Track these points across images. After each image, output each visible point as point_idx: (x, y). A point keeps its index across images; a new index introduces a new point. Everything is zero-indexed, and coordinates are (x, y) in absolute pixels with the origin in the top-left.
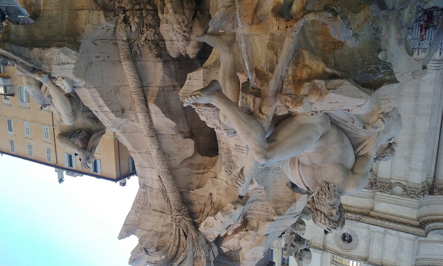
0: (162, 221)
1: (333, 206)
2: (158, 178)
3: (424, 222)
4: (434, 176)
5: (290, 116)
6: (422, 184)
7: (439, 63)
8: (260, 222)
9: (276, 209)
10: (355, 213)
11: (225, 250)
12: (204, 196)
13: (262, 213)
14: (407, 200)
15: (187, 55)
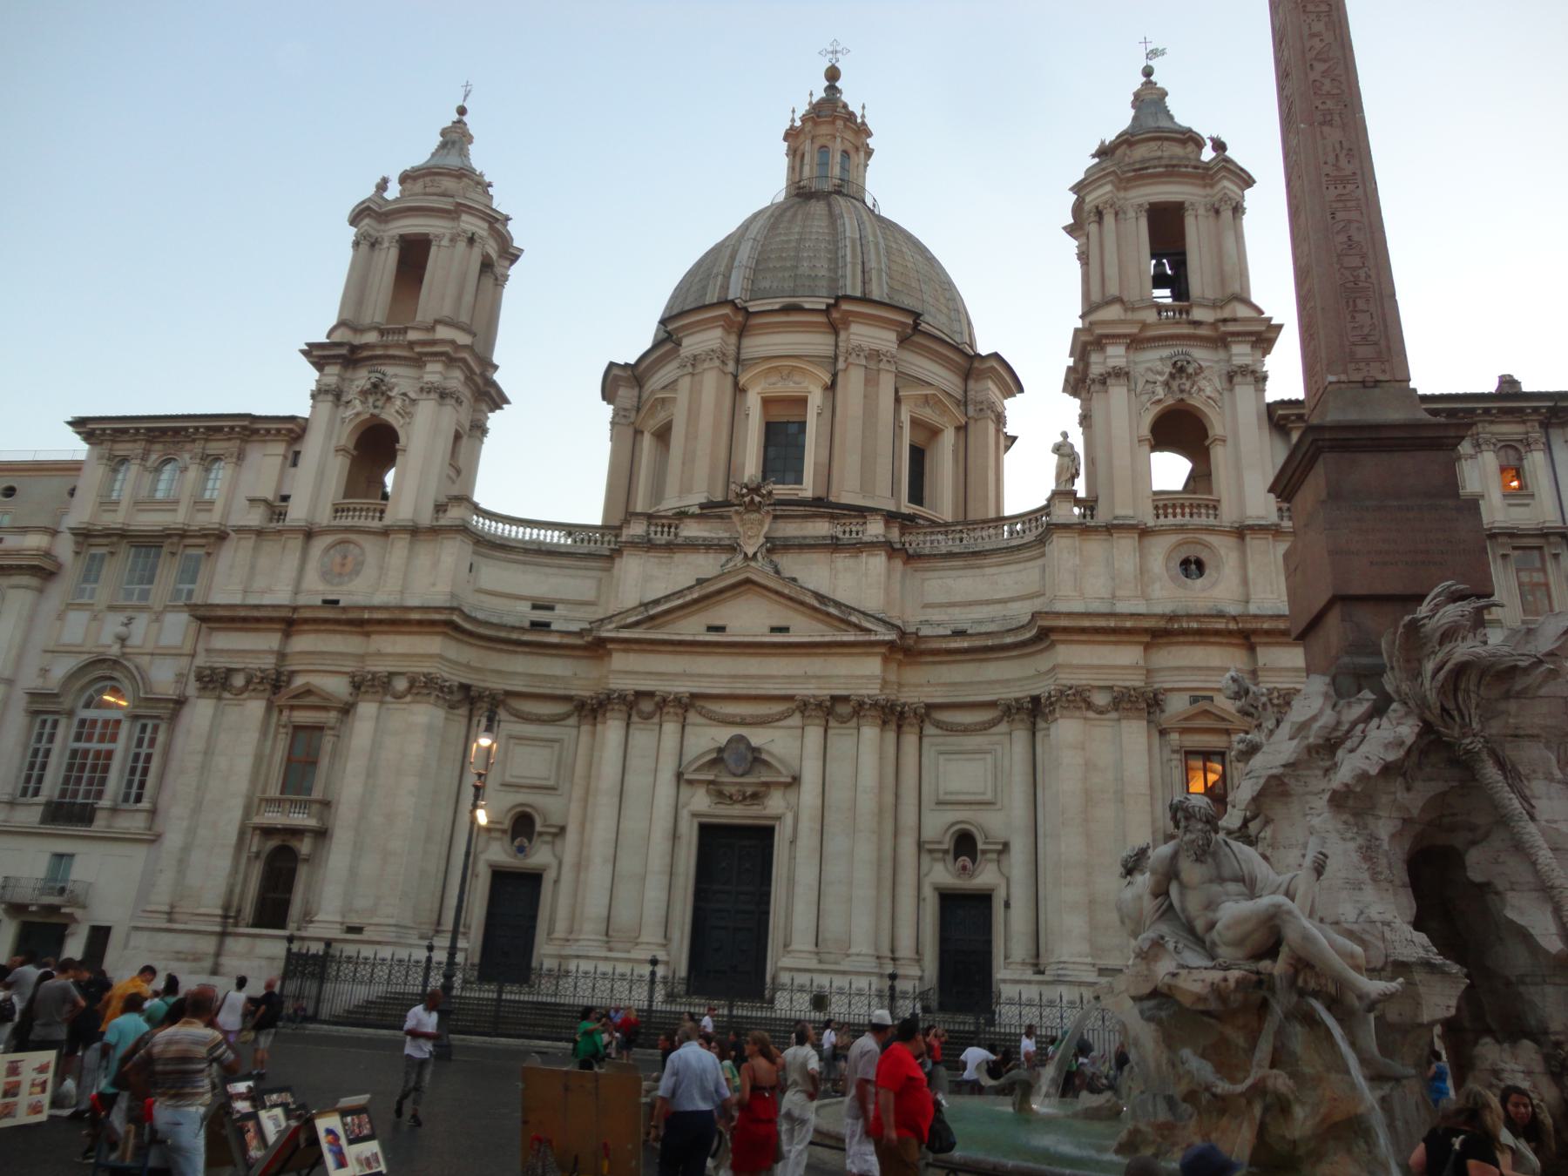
0: (1511, 721)
1: (1187, 829)
2: (1534, 802)
3: (1041, 640)
4: (1034, 734)
5: (1257, 956)
6: (1056, 719)
7: (1059, 975)
8: (1306, 757)
9: (1283, 784)
10: (1184, 632)
11: (1367, 694)
12: (1424, 781)
13: (1305, 773)
14: (1081, 679)
15: (1498, 1042)
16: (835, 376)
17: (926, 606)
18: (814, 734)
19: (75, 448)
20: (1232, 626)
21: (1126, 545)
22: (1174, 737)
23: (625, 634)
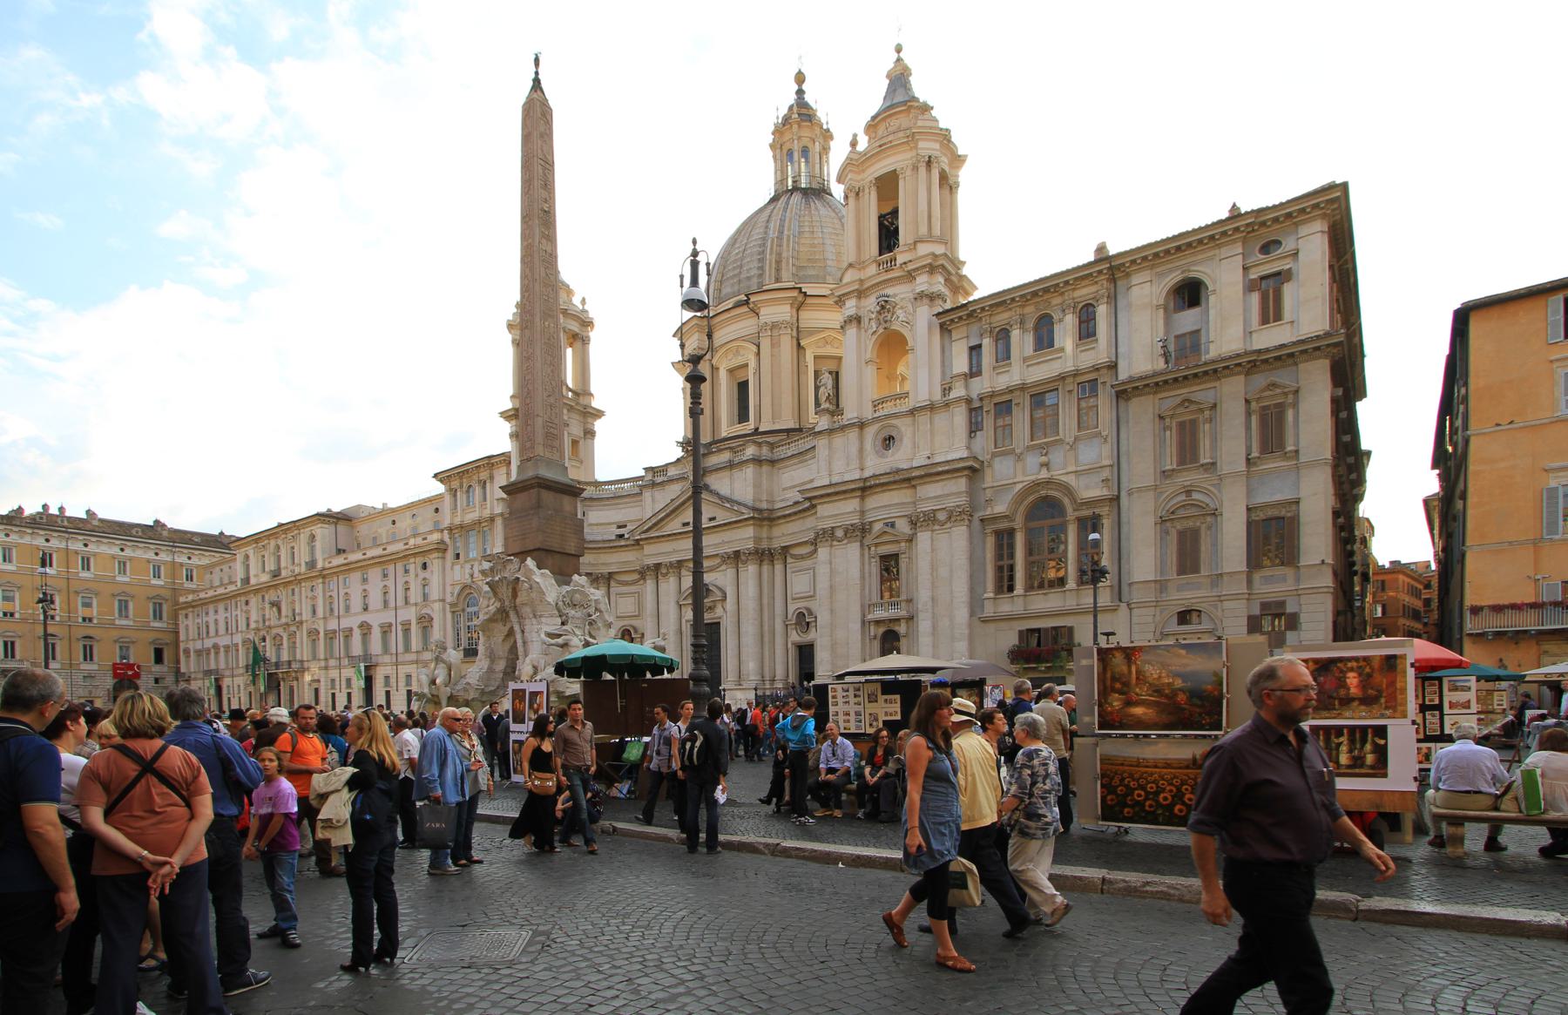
14: (828, 524)
16: (758, 346)
17: (784, 489)
18: (731, 572)
19: (439, 488)
20: (897, 478)
21: (853, 435)
22: (873, 548)
23: (643, 536)
